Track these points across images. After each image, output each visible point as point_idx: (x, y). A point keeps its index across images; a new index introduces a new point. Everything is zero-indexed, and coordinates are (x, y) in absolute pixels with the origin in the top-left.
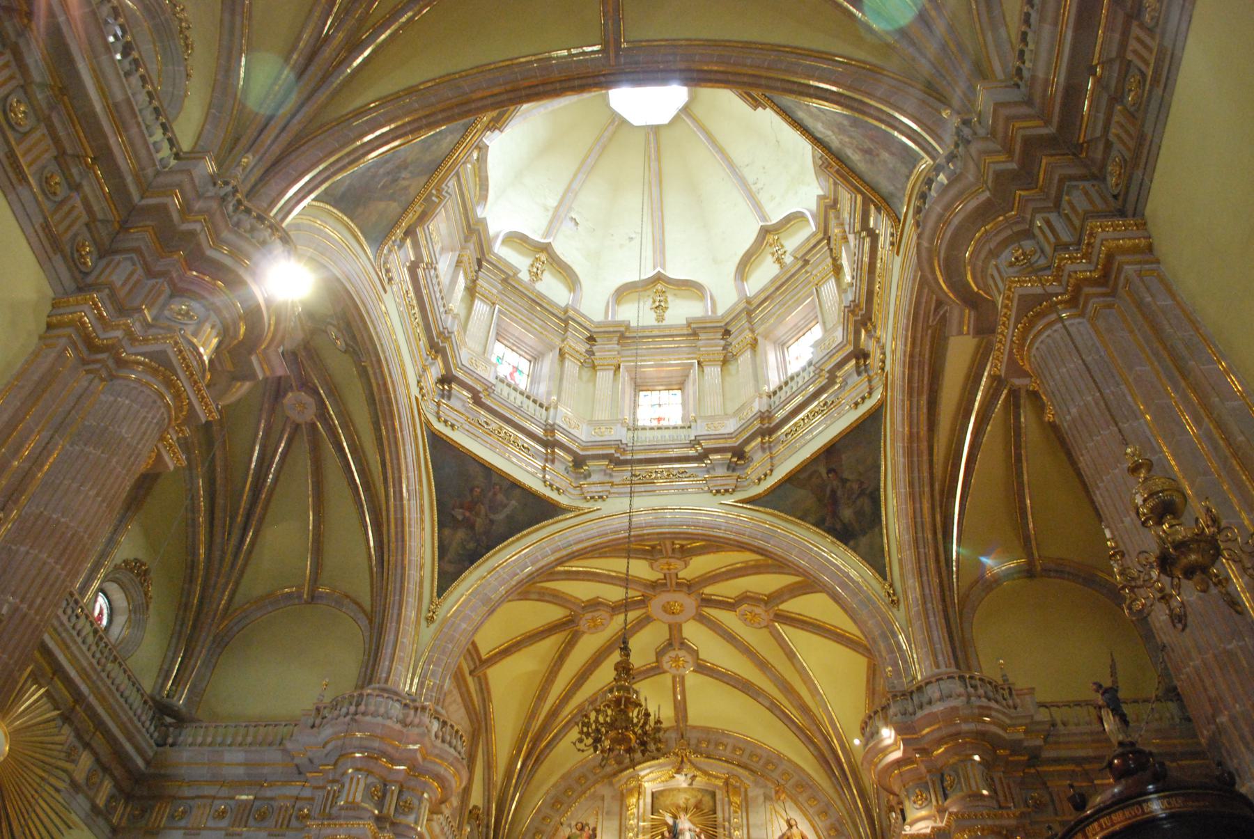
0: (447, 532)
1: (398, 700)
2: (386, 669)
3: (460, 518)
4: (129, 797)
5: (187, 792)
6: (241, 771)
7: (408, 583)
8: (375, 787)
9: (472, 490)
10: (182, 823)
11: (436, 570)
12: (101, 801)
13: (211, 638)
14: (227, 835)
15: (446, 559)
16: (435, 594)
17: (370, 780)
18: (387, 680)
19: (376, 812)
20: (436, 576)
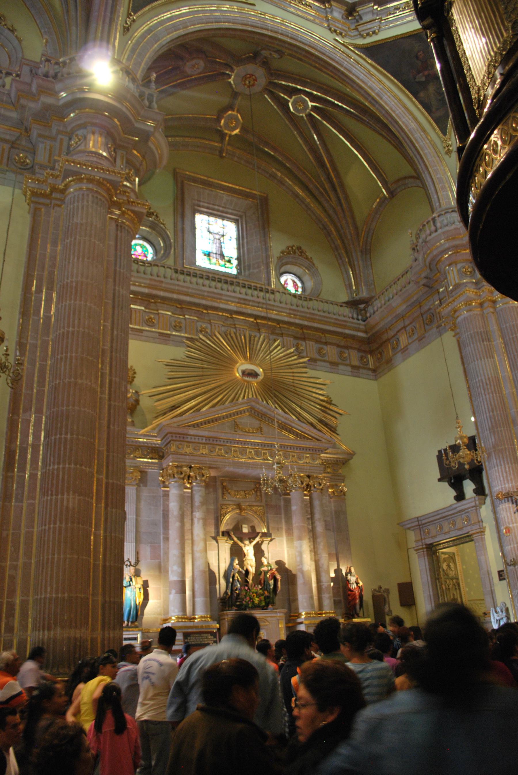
0: (422, 94)
1: (446, 213)
2: (436, 200)
3: (423, 79)
4: (371, 352)
5: (391, 333)
6: (404, 307)
7: (418, 143)
8: (464, 267)
9: (417, 57)
10: (399, 349)
11: (432, 121)
12: (356, 362)
13: (359, 253)
14: (419, 341)
15: (434, 109)
16: (441, 135)
17: (459, 266)
18: (440, 206)
19: (474, 281)
20: (434, 125)
